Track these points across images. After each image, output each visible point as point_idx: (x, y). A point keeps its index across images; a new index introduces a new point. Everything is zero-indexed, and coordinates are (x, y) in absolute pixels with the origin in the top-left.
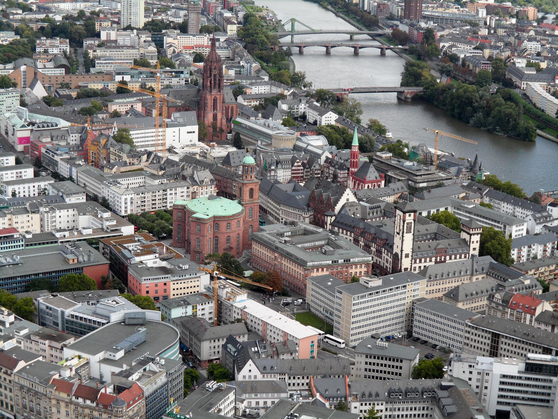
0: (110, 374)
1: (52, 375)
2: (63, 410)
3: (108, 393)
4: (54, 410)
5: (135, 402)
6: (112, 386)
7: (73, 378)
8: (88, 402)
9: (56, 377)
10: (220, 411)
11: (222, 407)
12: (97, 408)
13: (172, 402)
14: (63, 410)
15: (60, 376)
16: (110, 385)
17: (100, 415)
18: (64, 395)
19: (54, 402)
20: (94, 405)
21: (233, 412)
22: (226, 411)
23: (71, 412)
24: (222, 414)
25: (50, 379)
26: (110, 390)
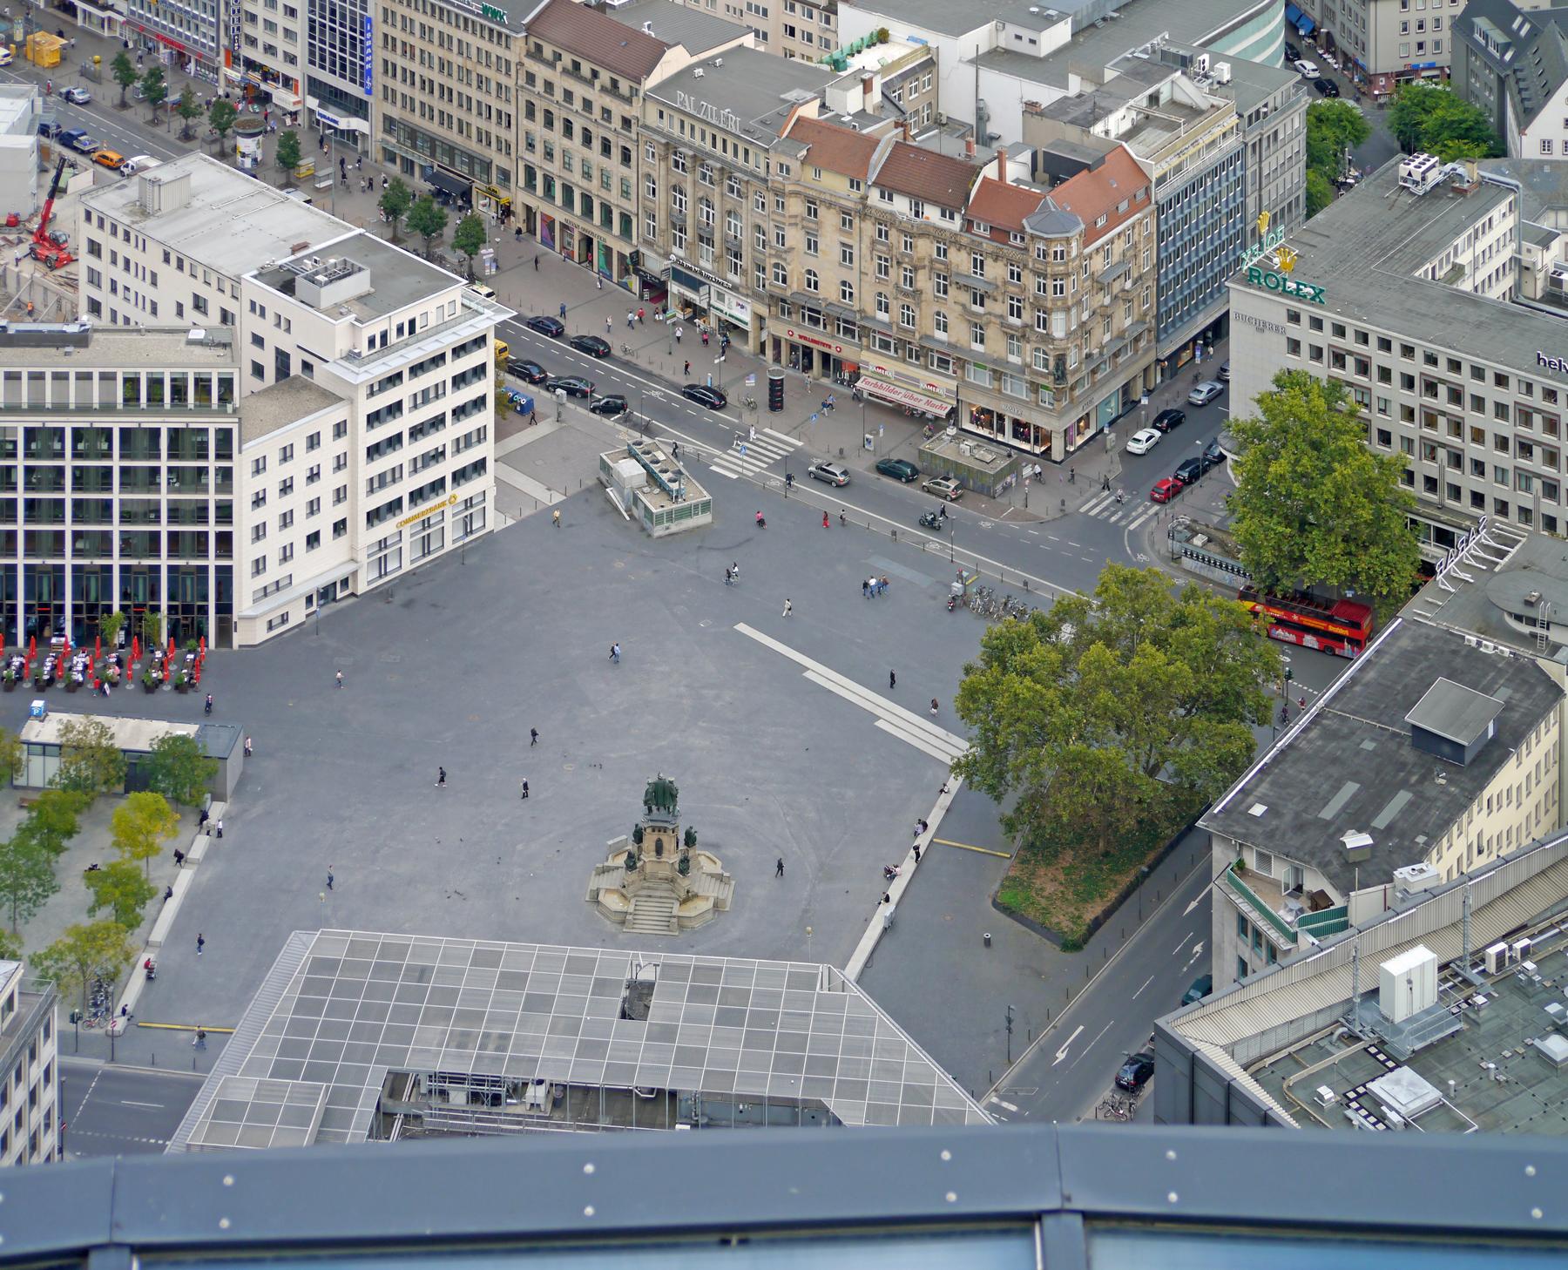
0: (1020, 108)
1: (794, 105)
2: (830, 239)
3: (1009, 180)
4: (795, 238)
5: (1115, 219)
6: (1026, 156)
7: (875, 119)
8: (932, 214)
9: (810, 111)
10: (1458, 271)
11: (1464, 259)
12: (965, 239)
13: (1264, 230)
14: (830, 239)
15: (823, 106)
16: (1017, 149)
17: (979, 265)
18: (835, 184)
19: (796, 207)
20: (956, 224)
21: (1508, 282)
22: (1482, 275)
23: (861, 249)
24: (1466, 286)
25: (783, 117)
26: (1016, 170)
